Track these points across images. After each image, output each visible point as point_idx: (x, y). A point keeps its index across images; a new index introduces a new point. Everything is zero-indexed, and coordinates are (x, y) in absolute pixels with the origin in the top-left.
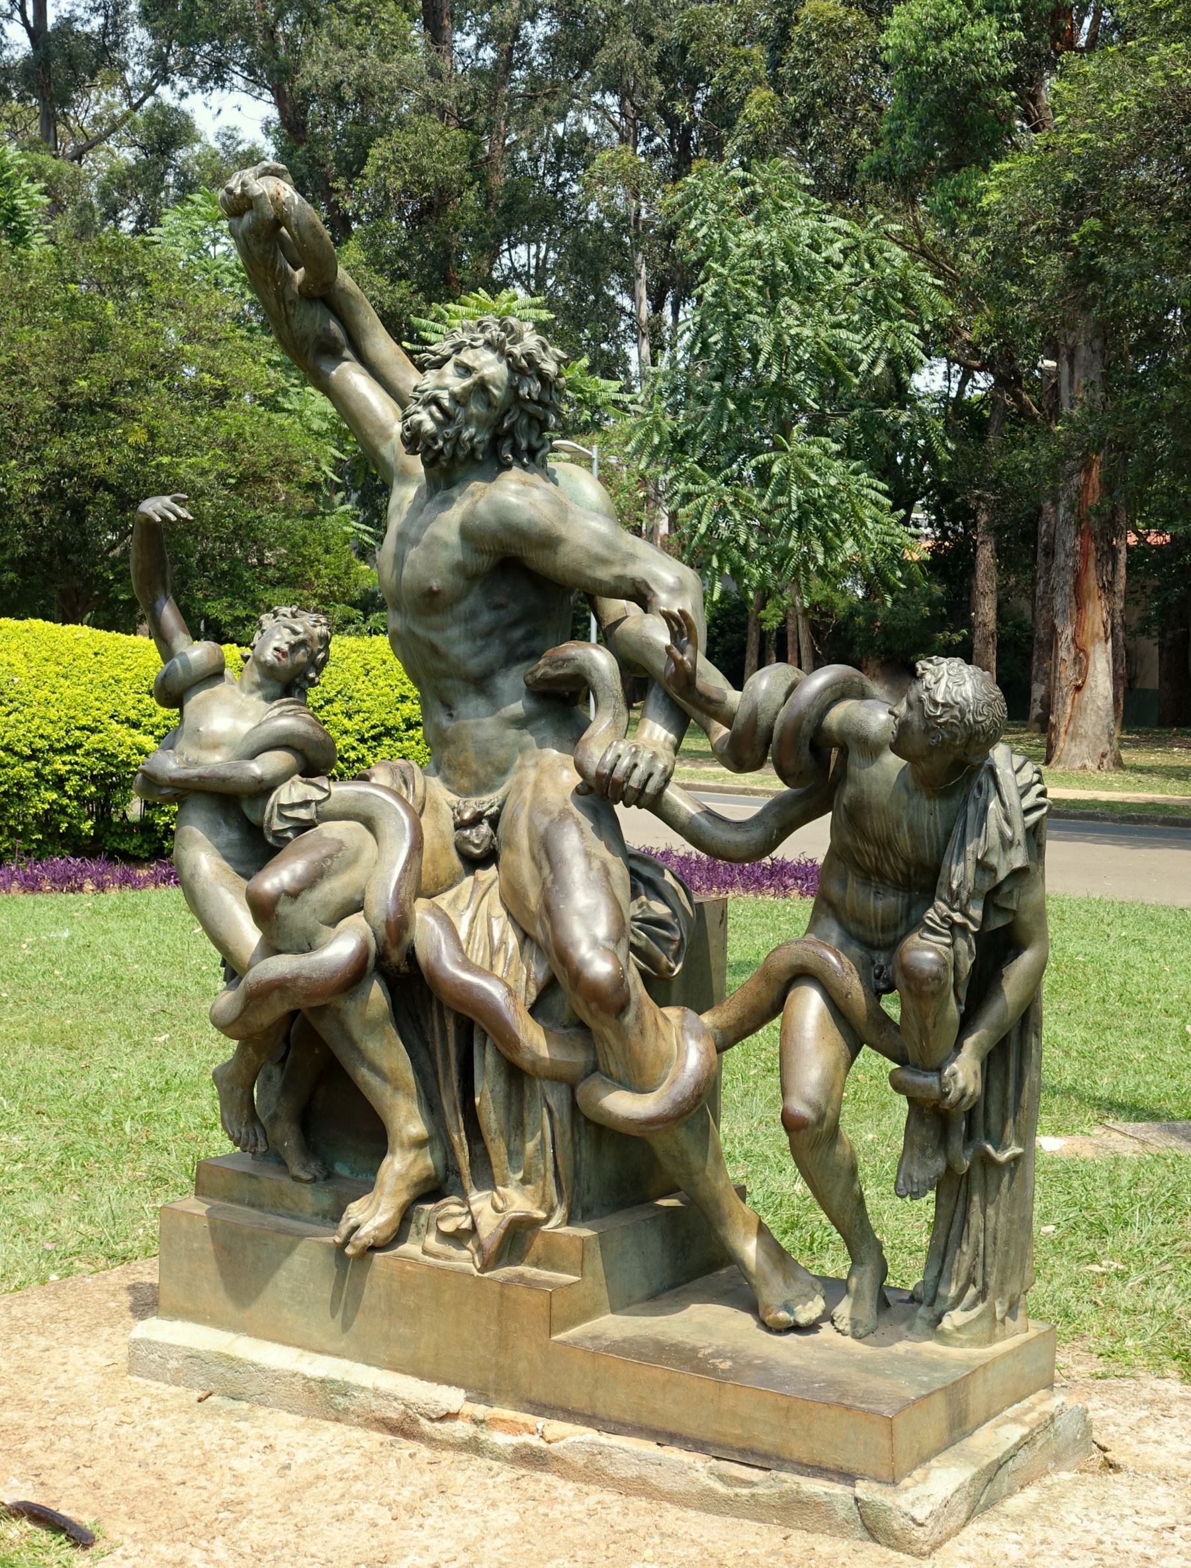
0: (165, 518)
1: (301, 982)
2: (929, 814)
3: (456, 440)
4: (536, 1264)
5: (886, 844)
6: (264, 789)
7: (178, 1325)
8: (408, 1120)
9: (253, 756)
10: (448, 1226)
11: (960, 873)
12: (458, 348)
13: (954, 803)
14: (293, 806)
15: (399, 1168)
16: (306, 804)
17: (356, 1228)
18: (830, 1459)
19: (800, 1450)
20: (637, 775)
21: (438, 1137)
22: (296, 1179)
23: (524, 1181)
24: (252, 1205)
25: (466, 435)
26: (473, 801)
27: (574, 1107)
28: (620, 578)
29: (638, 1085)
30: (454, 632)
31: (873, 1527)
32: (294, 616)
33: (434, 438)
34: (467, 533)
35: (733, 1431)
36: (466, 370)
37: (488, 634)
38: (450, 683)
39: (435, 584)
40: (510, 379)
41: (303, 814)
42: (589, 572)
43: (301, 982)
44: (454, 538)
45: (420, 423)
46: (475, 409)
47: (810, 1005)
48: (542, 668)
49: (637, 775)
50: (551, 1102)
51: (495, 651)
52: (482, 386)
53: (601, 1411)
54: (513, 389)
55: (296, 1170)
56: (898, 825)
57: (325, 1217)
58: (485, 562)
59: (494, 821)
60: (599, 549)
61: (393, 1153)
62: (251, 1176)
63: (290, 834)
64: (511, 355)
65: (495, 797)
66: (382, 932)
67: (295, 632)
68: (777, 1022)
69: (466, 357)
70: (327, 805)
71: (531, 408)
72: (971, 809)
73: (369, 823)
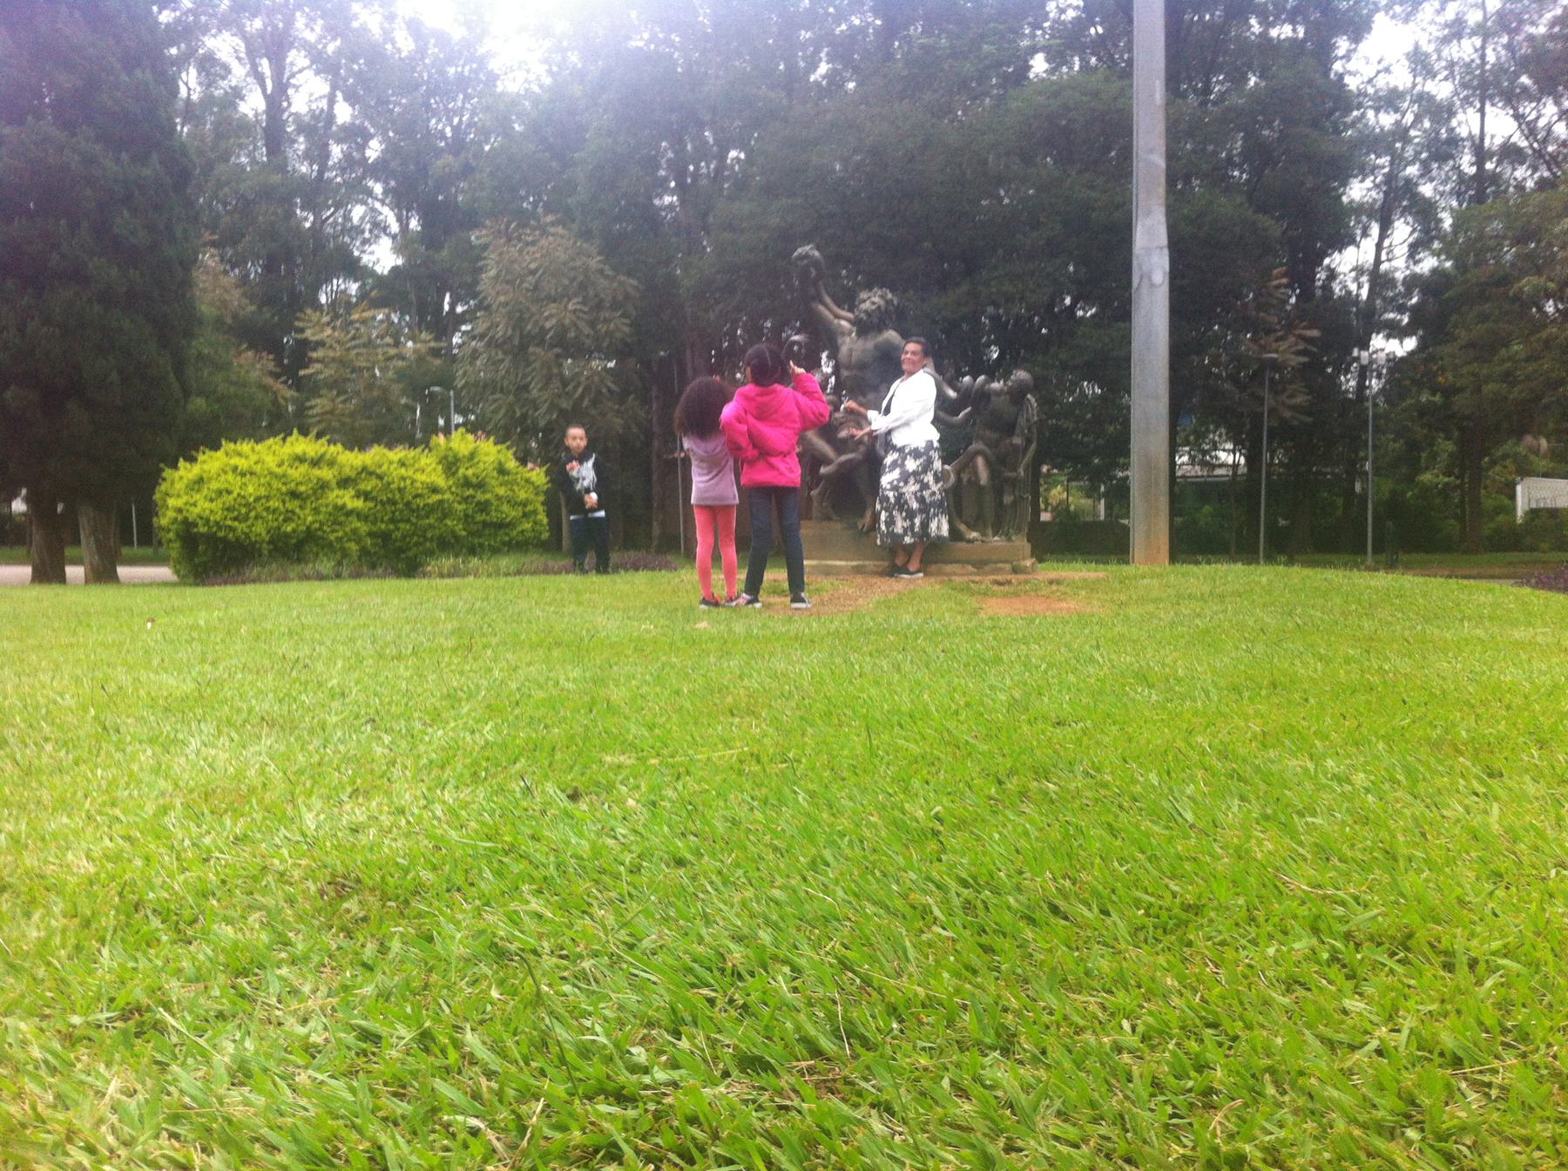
11: (1022, 421)
34: (876, 347)
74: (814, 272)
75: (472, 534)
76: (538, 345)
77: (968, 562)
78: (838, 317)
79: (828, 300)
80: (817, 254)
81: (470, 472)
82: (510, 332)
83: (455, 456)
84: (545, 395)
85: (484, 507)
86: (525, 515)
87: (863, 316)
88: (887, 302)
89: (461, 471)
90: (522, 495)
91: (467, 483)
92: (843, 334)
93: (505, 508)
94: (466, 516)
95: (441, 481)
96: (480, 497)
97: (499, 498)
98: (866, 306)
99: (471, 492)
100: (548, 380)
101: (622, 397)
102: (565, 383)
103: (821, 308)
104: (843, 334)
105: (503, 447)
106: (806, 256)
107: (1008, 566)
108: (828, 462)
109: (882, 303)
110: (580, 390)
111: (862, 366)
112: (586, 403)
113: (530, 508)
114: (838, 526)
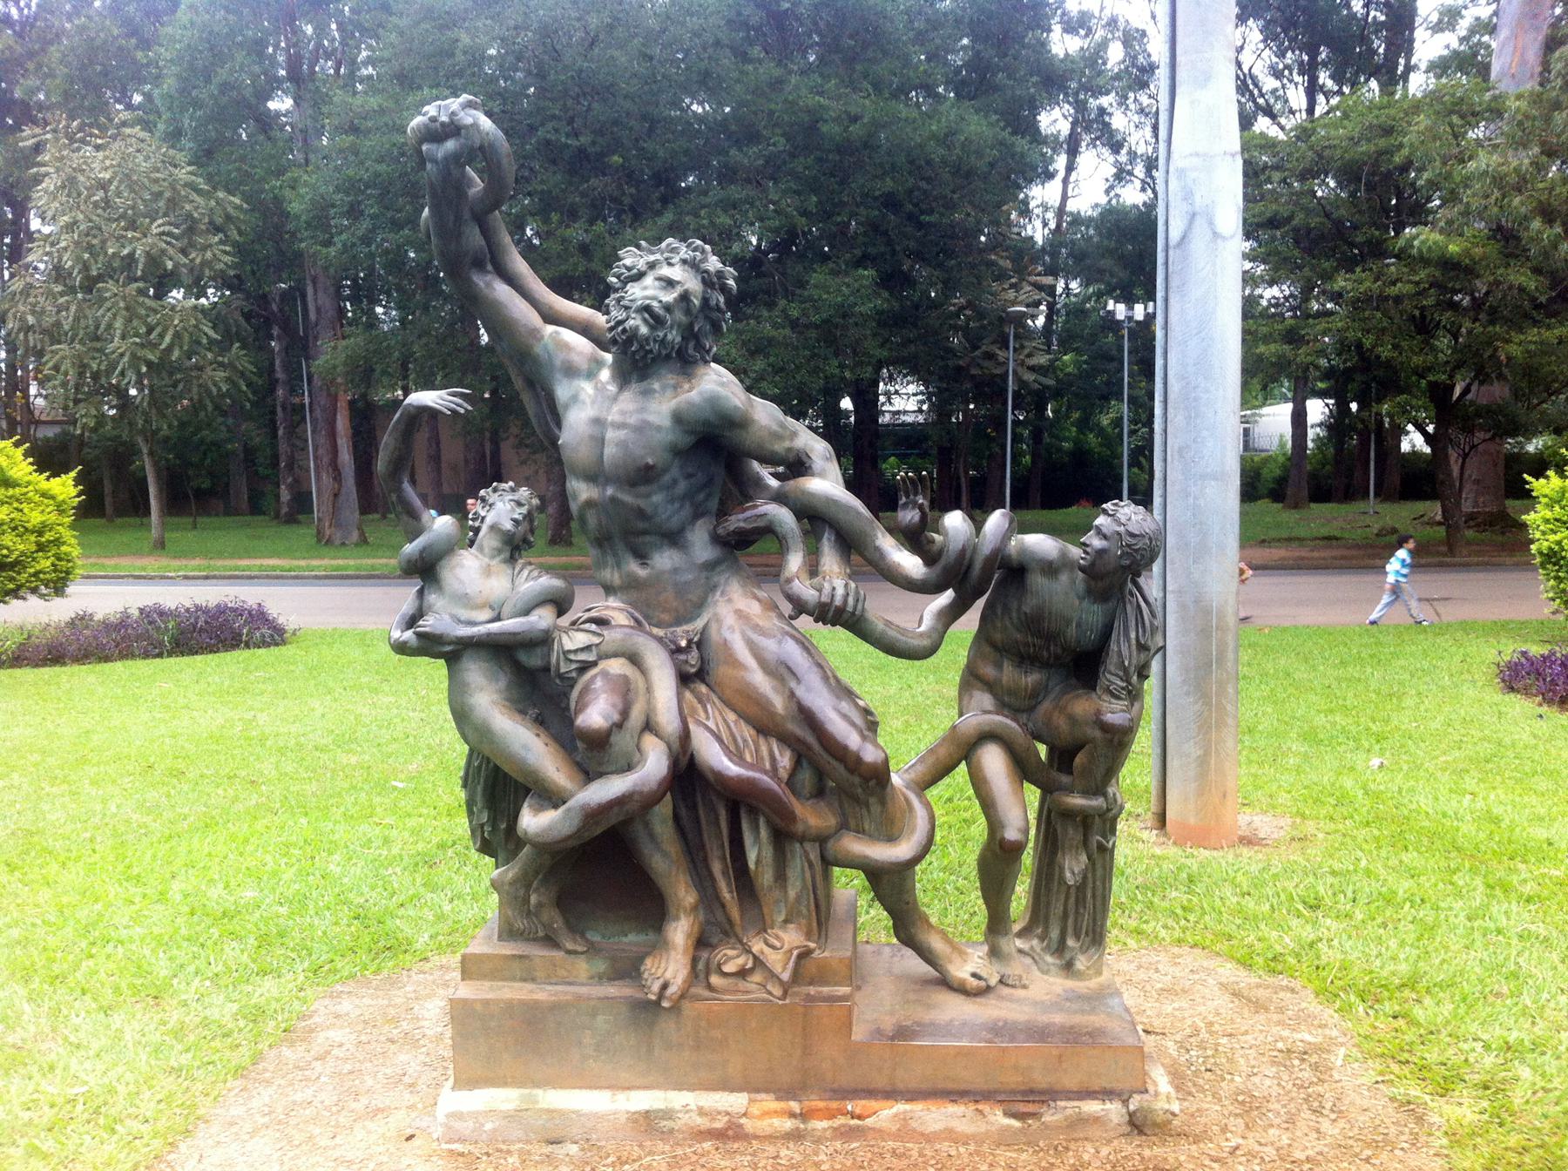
0: (454, 412)
1: (636, 797)
2: (1093, 614)
5: (1050, 637)
6: (543, 640)
8: (684, 893)
9: (527, 612)
10: (729, 968)
12: (652, 266)
14: (576, 651)
15: (680, 932)
16: (588, 648)
17: (665, 986)
18: (1096, 1084)
19: (1070, 1082)
20: (851, 601)
22: (569, 952)
23: (786, 921)
24: (524, 980)
25: (670, 337)
26: (679, 630)
28: (789, 450)
29: (891, 839)
30: (657, 498)
31: (1138, 1125)
32: (513, 490)
33: (647, 339)
34: (678, 418)
35: (1013, 1080)
36: (670, 283)
37: (684, 498)
38: (648, 538)
39: (650, 461)
40: (704, 292)
41: (582, 657)
42: (768, 446)
43: (636, 797)
44: (666, 422)
45: (637, 328)
46: (679, 316)
47: (994, 760)
49: (851, 601)
50: (812, 857)
51: (687, 511)
52: (685, 297)
53: (901, 1086)
54: (705, 301)
56: (1068, 622)
57: (600, 978)
58: (688, 440)
59: (699, 645)
60: (775, 427)
61: (677, 918)
62: (521, 957)
63: (574, 674)
64: (706, 271)
65: (699, 624)
66: (676, 746)
67: (519, 504)
69: (666, 271)
70: (603, 648)
71: (715, 315)
72: (1129, 607)
73: (634, 659)
74: (477, 185)
78: (551, 318)
79: (521, 266)
80: (486, 123)
86: (41, 547)
87: (636, 322)
88: (709, 281)
90: (35, 518)
92: (571, 371)
98: (644, 291)
101: (222, 346)
103: (502, 291)
104: (571, 371)
106: (452, 129)
107: (1113, 1110)
109: (693, 284)
110: (168, 339)
111: (642, 476)
112: (176, 354)
113: (48, 536)
114: (582, 967)
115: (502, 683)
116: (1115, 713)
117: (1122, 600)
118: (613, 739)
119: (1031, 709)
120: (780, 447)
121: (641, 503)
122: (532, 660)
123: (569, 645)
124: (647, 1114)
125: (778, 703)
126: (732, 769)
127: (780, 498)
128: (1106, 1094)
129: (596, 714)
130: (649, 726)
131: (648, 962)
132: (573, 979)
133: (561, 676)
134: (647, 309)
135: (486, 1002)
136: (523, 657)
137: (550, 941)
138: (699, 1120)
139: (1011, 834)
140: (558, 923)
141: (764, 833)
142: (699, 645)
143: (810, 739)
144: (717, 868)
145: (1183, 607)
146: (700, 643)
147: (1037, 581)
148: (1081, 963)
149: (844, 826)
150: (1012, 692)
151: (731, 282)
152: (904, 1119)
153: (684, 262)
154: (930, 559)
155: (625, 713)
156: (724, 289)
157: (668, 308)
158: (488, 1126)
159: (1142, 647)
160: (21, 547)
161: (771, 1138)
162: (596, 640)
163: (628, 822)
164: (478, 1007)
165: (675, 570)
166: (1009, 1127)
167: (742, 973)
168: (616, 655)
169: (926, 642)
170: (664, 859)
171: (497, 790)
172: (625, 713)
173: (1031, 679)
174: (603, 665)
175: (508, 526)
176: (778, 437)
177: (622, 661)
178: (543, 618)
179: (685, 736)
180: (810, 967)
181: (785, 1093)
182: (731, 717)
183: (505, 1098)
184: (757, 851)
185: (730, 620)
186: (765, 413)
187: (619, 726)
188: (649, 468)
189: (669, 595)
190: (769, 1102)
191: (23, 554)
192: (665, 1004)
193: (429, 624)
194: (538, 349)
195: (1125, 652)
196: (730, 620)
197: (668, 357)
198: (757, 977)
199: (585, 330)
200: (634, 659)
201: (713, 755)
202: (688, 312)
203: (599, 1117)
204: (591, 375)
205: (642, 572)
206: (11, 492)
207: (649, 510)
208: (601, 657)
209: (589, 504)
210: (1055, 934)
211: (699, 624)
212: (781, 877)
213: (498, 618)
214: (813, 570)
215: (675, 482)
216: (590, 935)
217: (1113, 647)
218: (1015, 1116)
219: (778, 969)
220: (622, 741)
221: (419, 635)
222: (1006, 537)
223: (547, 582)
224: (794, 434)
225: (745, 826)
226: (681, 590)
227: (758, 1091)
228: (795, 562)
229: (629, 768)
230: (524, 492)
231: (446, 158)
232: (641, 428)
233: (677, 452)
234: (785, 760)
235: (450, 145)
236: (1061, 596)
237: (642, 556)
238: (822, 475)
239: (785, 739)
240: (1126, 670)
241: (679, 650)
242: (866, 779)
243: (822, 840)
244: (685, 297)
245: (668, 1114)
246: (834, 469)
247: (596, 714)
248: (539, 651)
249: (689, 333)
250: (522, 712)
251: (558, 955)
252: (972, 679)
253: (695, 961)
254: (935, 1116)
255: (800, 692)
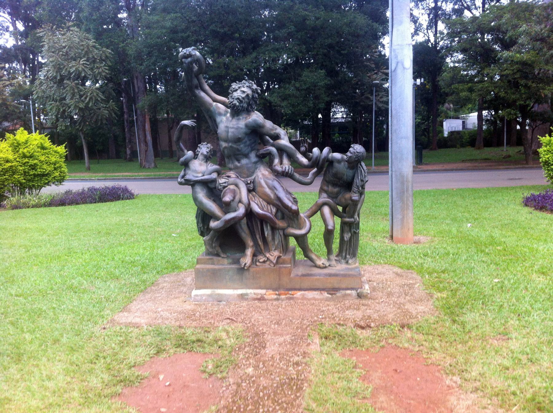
2: (350, 173)
3: (242, 106)
4: (281, 264)
5: (340, 179)
6: (214, 181)
7: (202, 290)
9: (210, 174)
10: (261, 261)
12: (239, 88)
13: (354, 170)
15: (249, 252)
16: (225, 183)
17: (245, 264)
18: (350, 287)
19: (344, 286)
21: (256, 244)
23: (275, 249)
27: (284, 234)
29: (300, 228)
30: (242, 146)
33: (238, 106)
34: (246, 126)
35: (330, 286)
36: (244, 92)
37: (248, 146)
41: (224, 185)
46: (246, 100)
48: (262, 151)
51: (250, 148)
52: (248, 95)
53: (302, 287)
54: (253, 96)
55: (222, 256)
58: (249, 131)
65: (253, 177)
66: (247, 206)
68: (319, 213)
69: (243, 89)
73: (237, 185)
74: (196, 68)
75: (29, 181)
76: (68, 80)
77: (324, 290)
78: (215, 100)
79: (207, 88)
80: (198, 53)
81: (25, 151)
82: (55, 74)
83: (17, 143)
84: (73, 102)
85: (33, 167)
86: (55, 169)
87: (235, 102)
88: (254, 91)
89: (21, 150)
90: (53, 159)
91: (25, 156)
92: (220, 114)
93: (45, 166)
94: (25, 172)
95: (11, 157)
96: (32, 162)
97: (41, 162)
98: (236, 94)
99: (27, 160)
100: (73, 95)
101: (107, 101)
102: (81, 96)
103: (203, 94)
104: (220, 114)
105: (43, 135)
106: (190, 56)
107: (354, 293)
108: (217, 218)
109: (249, 92)
110: (88, 99)
111: (238, 140)
112: (90, 104)
113: (57, 165)
114: (226, 261)
115: (205, 191)
116: (355, 197)
117: (357, 169)
118: (232, 203)
119: (336, 198)
120: (272, 132)
121: (238, 147)
122: (212, 186)
123: (220, 182)
124: (242, 294)
125: (272, 196)
126: (260, 211)
127: (273, 145)
128: (352, 289)
129: (227, 198)
130: (240, 201)
131: (241, 259)
132: (224, 264)
133: (219, 190)
134: (238, 99)
135: (203, 269)
136: (210, 185)
137: (218, 255)
138: (254, 296)
139: (330, 227)
140: (220, 251)
141: (269, 227)
142: (253, 182)
143: (280, 204)
144: (258, 237)
145: (396, 175)
146: (253, 182)
147: (336, 165)
148: (350, 261)
149: (289, 226)
150: (332, 193)
151: (259, 91)
152: (303, 295)
153: (247, 86)
154: (309, 159)
155: (234, 198)
156: (258, 93)
157: (243, 98)
158: (204, 298)
159: (362, 181)
160: (49, 169)
161: (271, 300)
162: (227, 181)
163: (236, 223)
164: (201, 270)
165: (247, 164)
166: (328, 297)
167: (264, 262)
168: (232, 184)
169: (309, 181)
170: (245, 234)
171: (204, 217)
172: (234, 198)
173: (336, 190)
174: (229, 187)
175: (205, 153)
176: (272, 130)
177: (234, 186)
178: (214, 175)
179: (249, 204)
180: (281, 260)
181: (275, 289)
182: (261, 200)
183: (208, 292)
184: (268, 232)
185: (260, 176)
186: (269, 124)
187: (233, 200)
188: (239, 138)
189: (245, 170)
190: (271, 292)
191: (50, 171)
192: (246, 268)
193: (187, 177)
194: (212, 109)
195: (358, 182)
196: (260, 176)
197: (244, 110)
198: (268, 263)
199: (223, 103)
200: (237, 185)
201: (256, 208)
202: (248, 99)
203: (230, 295)
204: (225, 115)
205: (239, 165)
206: (45, 151)
207: (240, 149)
208: (229, 185)
209: (225, 148)
210: (344, 254)
211: (253, 177)
212: (273, 239)
213: (204, 176)
214: (281, 163)
215: (246, 142)
216: (228, 254)
217: (355, 180)
218: (330, 294)
219: (273, 260)
220: (234, 204)
221: (185, 180)
222: (328, 154)
223: (216, 167)
224: (276, 129)
225: (264, 226)
226: (248, 169)
227: (268, 289)
228: (277, 161)
229: (235, 211)
230: (209, 145)
231: (188, 63)
232: (238, 128)
233: (246, 134)
234: (274, 210)
235: (189, 59)
236: (342, 168)
237: (239, 161)
238: (283, 139)
239: (274, 205)
240: (358, 186)
241: (248, 184)
242: (293, 213)
243: (283, 229)
244: (248, 95)
245: (247, 294)
246: (286, 138)
247: (227, 198)
248: (214, 184)
249: (249, 104)
250: (210, 199)
251: (220, 258)
252: (322, 190)
253: (253, 259)
254: (310, 294)
255: (277, 193)
